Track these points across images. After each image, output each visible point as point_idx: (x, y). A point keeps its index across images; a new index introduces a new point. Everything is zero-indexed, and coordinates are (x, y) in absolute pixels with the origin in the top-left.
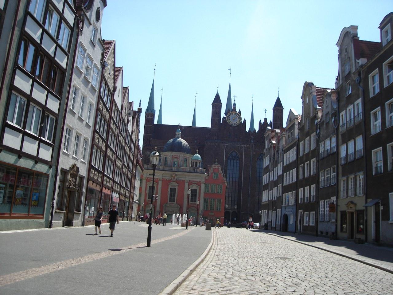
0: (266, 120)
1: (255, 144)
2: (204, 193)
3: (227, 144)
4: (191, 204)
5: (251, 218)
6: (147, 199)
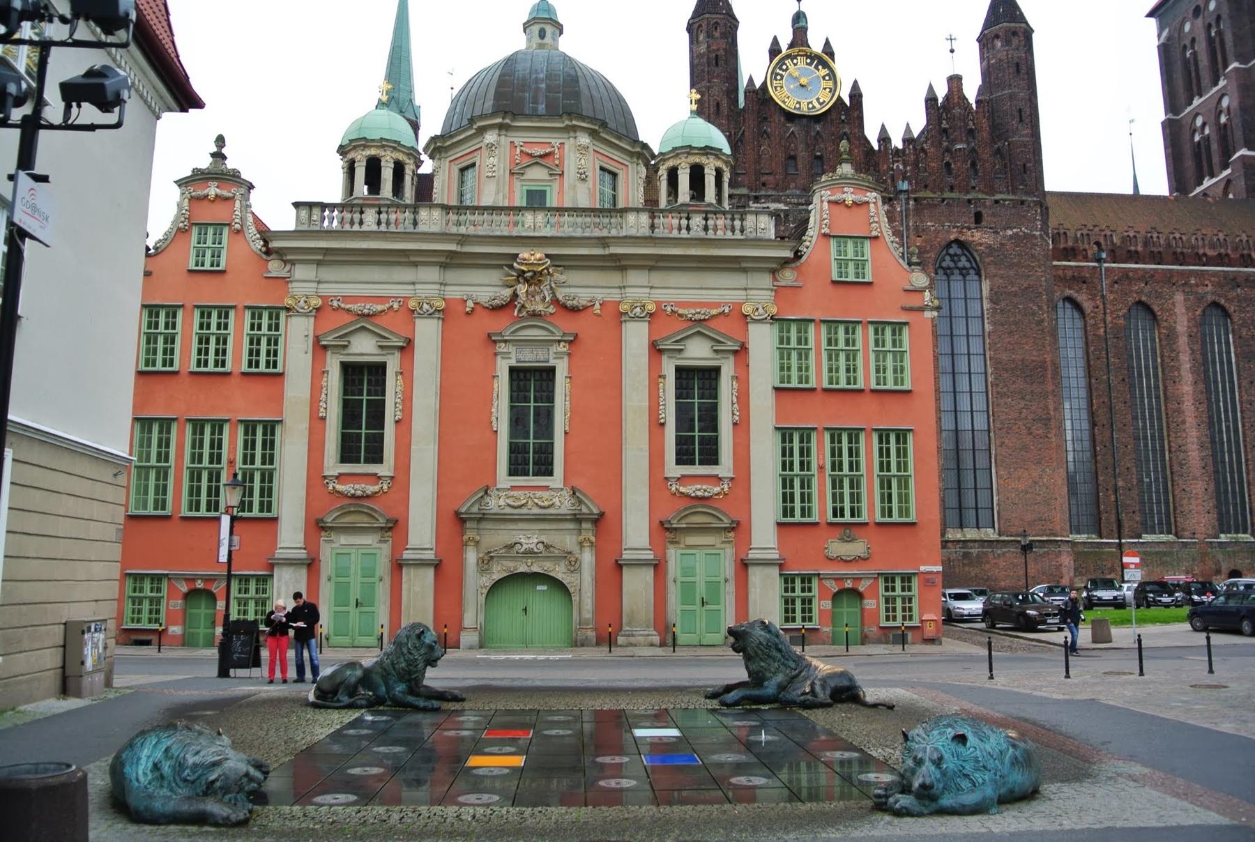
0: (955, 82)
1: (916, 200)
2: (777, 389)
3: (782, 206)
4: (682, 479)
5: (1137, 560)
6: (332, 465)
